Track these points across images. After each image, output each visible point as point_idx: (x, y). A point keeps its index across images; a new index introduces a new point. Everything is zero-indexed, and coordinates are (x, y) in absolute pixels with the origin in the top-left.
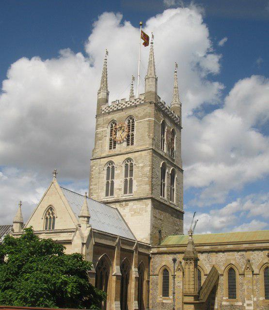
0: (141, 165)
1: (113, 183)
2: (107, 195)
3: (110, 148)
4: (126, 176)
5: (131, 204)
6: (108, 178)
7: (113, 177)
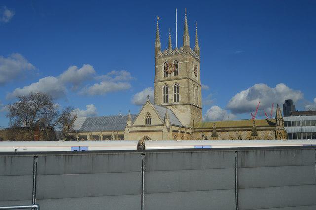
0: (183, 87)
1: (167, 96)
2: (165, 102)
3: (165, 77)
4: (175, 92)
5: (179, 107)
6: (165, 93)
7: (167, 93)
